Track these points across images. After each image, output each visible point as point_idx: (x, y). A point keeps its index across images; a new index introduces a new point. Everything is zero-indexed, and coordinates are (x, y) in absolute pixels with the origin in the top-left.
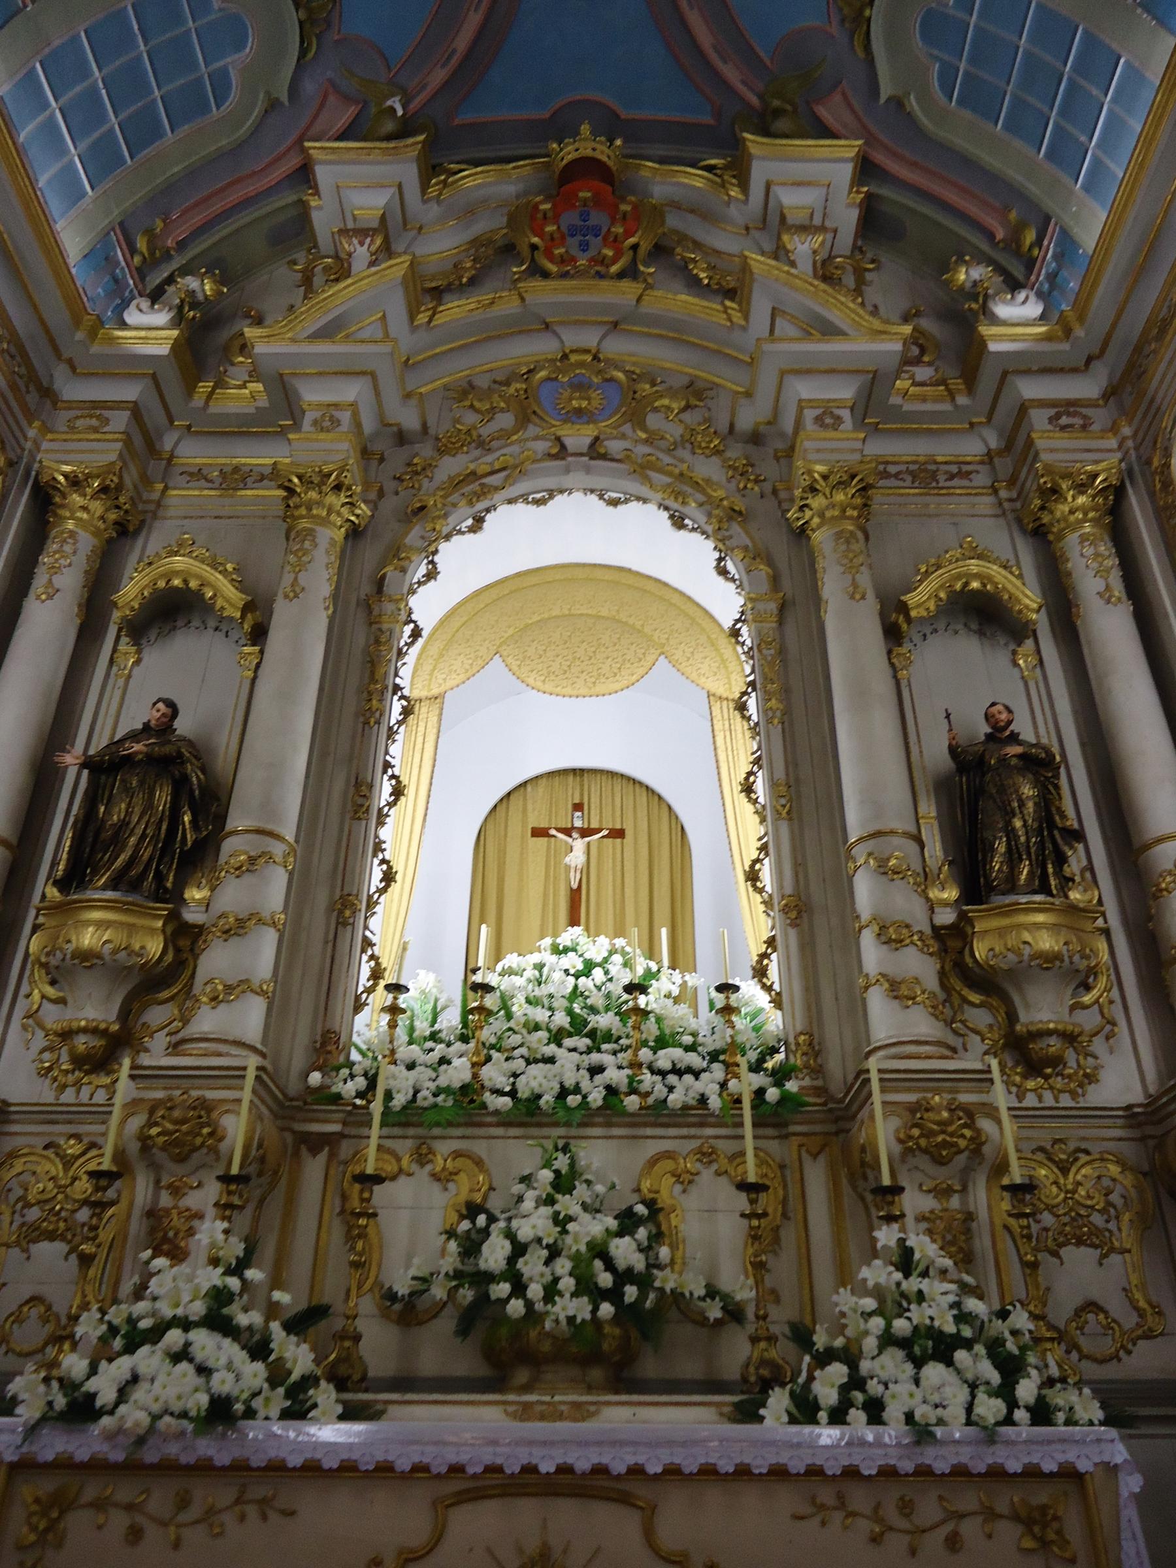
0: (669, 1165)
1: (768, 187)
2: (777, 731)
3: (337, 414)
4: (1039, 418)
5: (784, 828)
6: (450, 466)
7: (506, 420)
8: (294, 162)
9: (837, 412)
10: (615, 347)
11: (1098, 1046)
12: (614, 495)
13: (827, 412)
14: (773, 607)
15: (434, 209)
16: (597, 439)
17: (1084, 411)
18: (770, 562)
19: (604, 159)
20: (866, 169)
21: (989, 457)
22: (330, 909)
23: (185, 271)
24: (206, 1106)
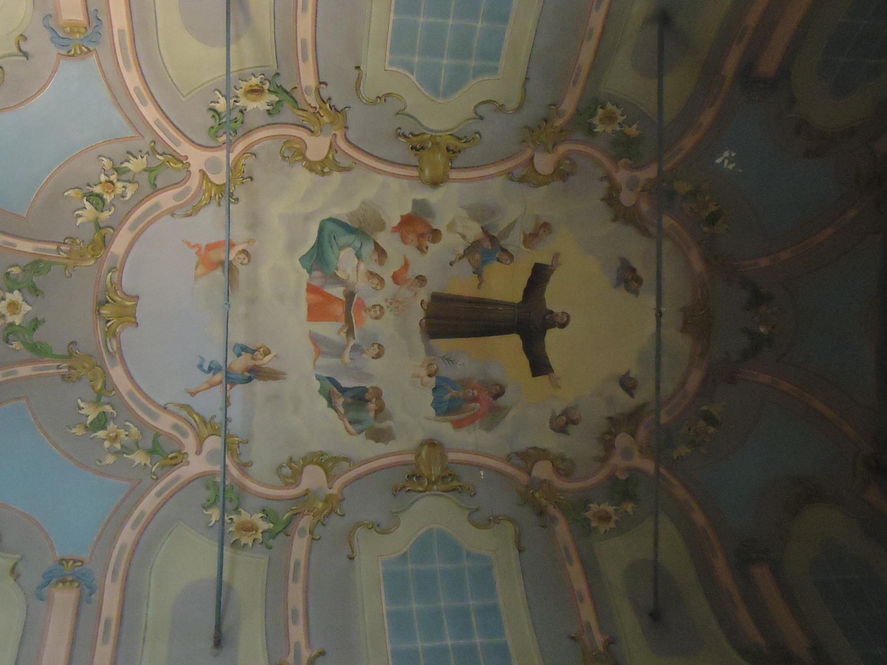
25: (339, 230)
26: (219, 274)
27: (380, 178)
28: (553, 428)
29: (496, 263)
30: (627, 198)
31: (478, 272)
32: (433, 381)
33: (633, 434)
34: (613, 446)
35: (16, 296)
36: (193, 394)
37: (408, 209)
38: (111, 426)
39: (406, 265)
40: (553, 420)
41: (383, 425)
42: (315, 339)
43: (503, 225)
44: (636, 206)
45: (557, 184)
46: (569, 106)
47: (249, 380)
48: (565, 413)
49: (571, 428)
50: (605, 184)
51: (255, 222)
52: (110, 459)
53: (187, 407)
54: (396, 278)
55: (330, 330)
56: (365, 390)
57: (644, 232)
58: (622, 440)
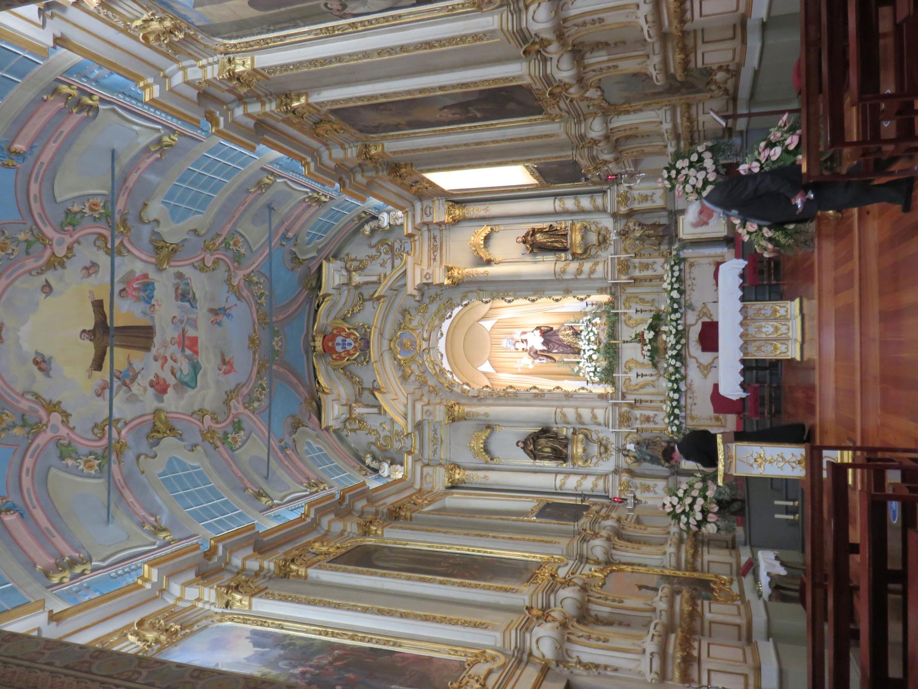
0: (627, 322)
1: (333, 288)
2: (518, 294)
3: (425, 411)
4: (426, 219)
5: (546, 293)
6: (431, 382)
7: (414, 367)
8: (325, 432)
9: (425, 274)
10: (387, 335)
11: (600, 226)
12: (439, 334)
13: (425, 277)
14: (482, 293)
15: (334, 391)
16: (423, 339)
17: (424, 207)
18: (467, 292)
19: (321, 339)
20: (327, 259)
21: (429, 230)
22: (567, 400)
23: (364, 463)
24: (620, 415)
25: (190, 384)
26: (227, 359)
27: (180, 411)
28: (98, 266)
29: (121, 370)
30: (56, 418)
31: (130, 364)
32: (153, 302)
33: (54, 253)
34: (68, 249)
35: (277, 348)
36: (236, 305)
37: (165, 397)
38: (259, 293)
39: (162, 366)
40: (96, 272)
41: (177, 281)
42: (195, 327)
43: (121, 393)
44: (49, 414)
45: (99, 421)
46: (115, 467)
47: (219, 309)
48: (89, 275)
49: (88, 264)
50: (71, 425)
51: (218, 383)
52: (262, 281)
53: (239, 299)
54: (166, 360)
55: (191, 333)
56: (182, 300)
57: (37, 396)
58: (61, 252)
